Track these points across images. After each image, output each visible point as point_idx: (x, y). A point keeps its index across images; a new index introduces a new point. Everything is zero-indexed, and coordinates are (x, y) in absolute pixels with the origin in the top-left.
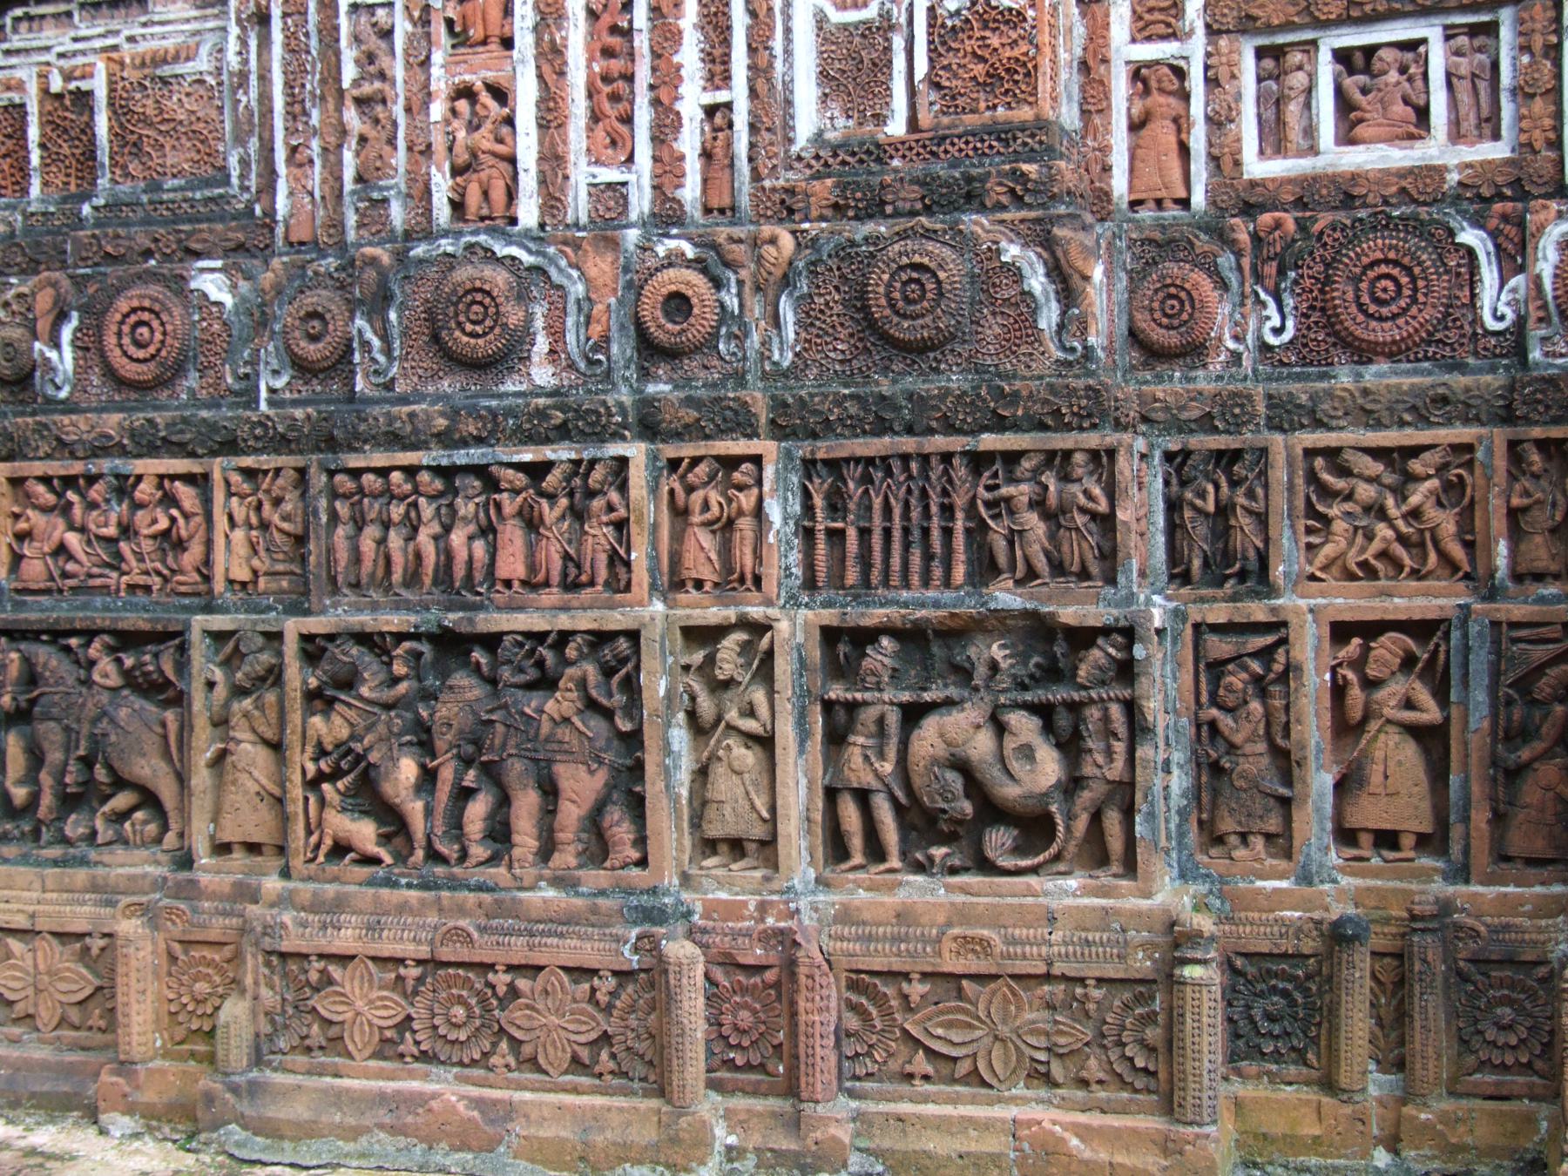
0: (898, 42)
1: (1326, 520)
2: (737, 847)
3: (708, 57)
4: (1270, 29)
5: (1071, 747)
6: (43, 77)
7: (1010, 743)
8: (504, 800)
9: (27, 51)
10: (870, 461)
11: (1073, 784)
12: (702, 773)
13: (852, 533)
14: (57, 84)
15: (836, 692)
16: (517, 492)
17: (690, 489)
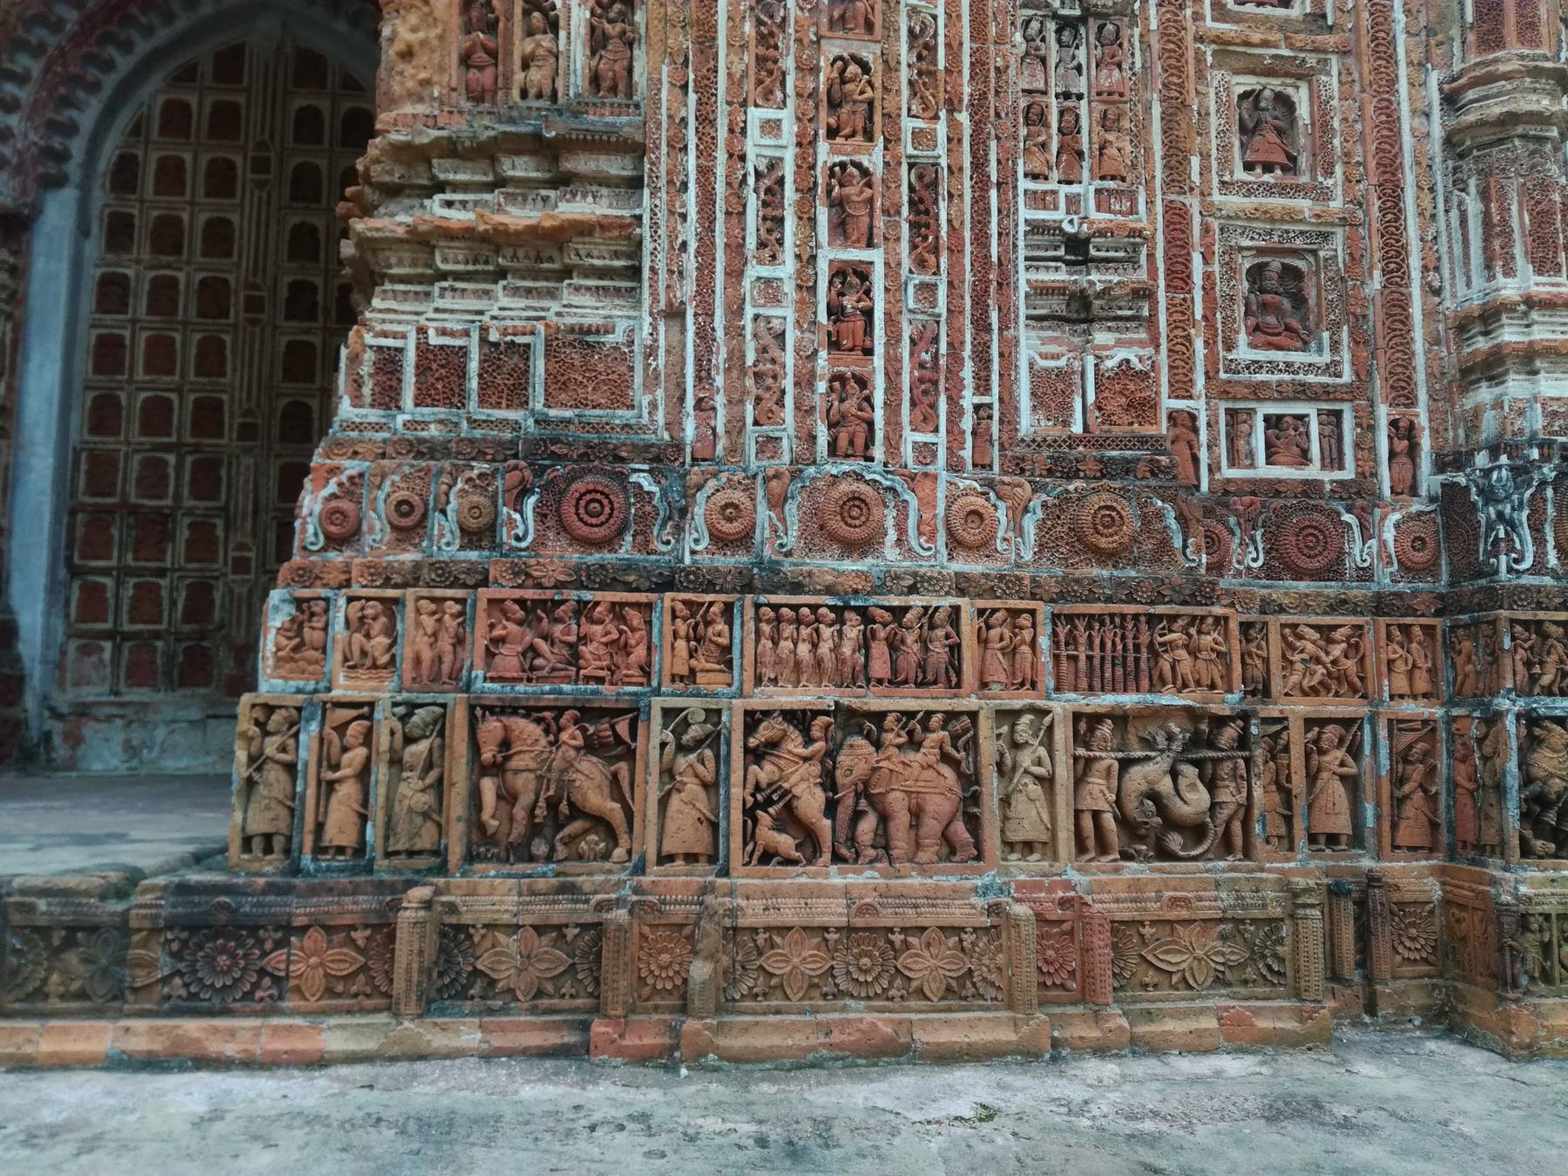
0: (1077, 379)
1: (1292, 663)
2: (1028, 847)
3: (977, 376)
4: (1235, 399)
5: (1212, 785)
6: (422, 331)
7: (1182, 782)
8: (884, 818)
9: (452, 311)
10: (1092, 616)
11: (1214, 806)
12: (1006, 802)
13: (1083, 657)
14: (494, 336)
15: (1081, 752)
16: (885, 625)
17: (989, 627)
